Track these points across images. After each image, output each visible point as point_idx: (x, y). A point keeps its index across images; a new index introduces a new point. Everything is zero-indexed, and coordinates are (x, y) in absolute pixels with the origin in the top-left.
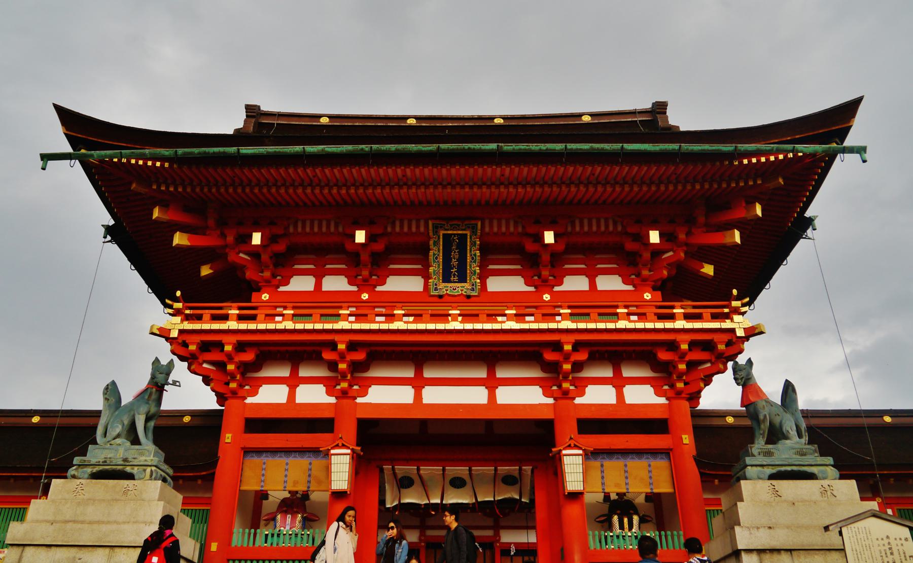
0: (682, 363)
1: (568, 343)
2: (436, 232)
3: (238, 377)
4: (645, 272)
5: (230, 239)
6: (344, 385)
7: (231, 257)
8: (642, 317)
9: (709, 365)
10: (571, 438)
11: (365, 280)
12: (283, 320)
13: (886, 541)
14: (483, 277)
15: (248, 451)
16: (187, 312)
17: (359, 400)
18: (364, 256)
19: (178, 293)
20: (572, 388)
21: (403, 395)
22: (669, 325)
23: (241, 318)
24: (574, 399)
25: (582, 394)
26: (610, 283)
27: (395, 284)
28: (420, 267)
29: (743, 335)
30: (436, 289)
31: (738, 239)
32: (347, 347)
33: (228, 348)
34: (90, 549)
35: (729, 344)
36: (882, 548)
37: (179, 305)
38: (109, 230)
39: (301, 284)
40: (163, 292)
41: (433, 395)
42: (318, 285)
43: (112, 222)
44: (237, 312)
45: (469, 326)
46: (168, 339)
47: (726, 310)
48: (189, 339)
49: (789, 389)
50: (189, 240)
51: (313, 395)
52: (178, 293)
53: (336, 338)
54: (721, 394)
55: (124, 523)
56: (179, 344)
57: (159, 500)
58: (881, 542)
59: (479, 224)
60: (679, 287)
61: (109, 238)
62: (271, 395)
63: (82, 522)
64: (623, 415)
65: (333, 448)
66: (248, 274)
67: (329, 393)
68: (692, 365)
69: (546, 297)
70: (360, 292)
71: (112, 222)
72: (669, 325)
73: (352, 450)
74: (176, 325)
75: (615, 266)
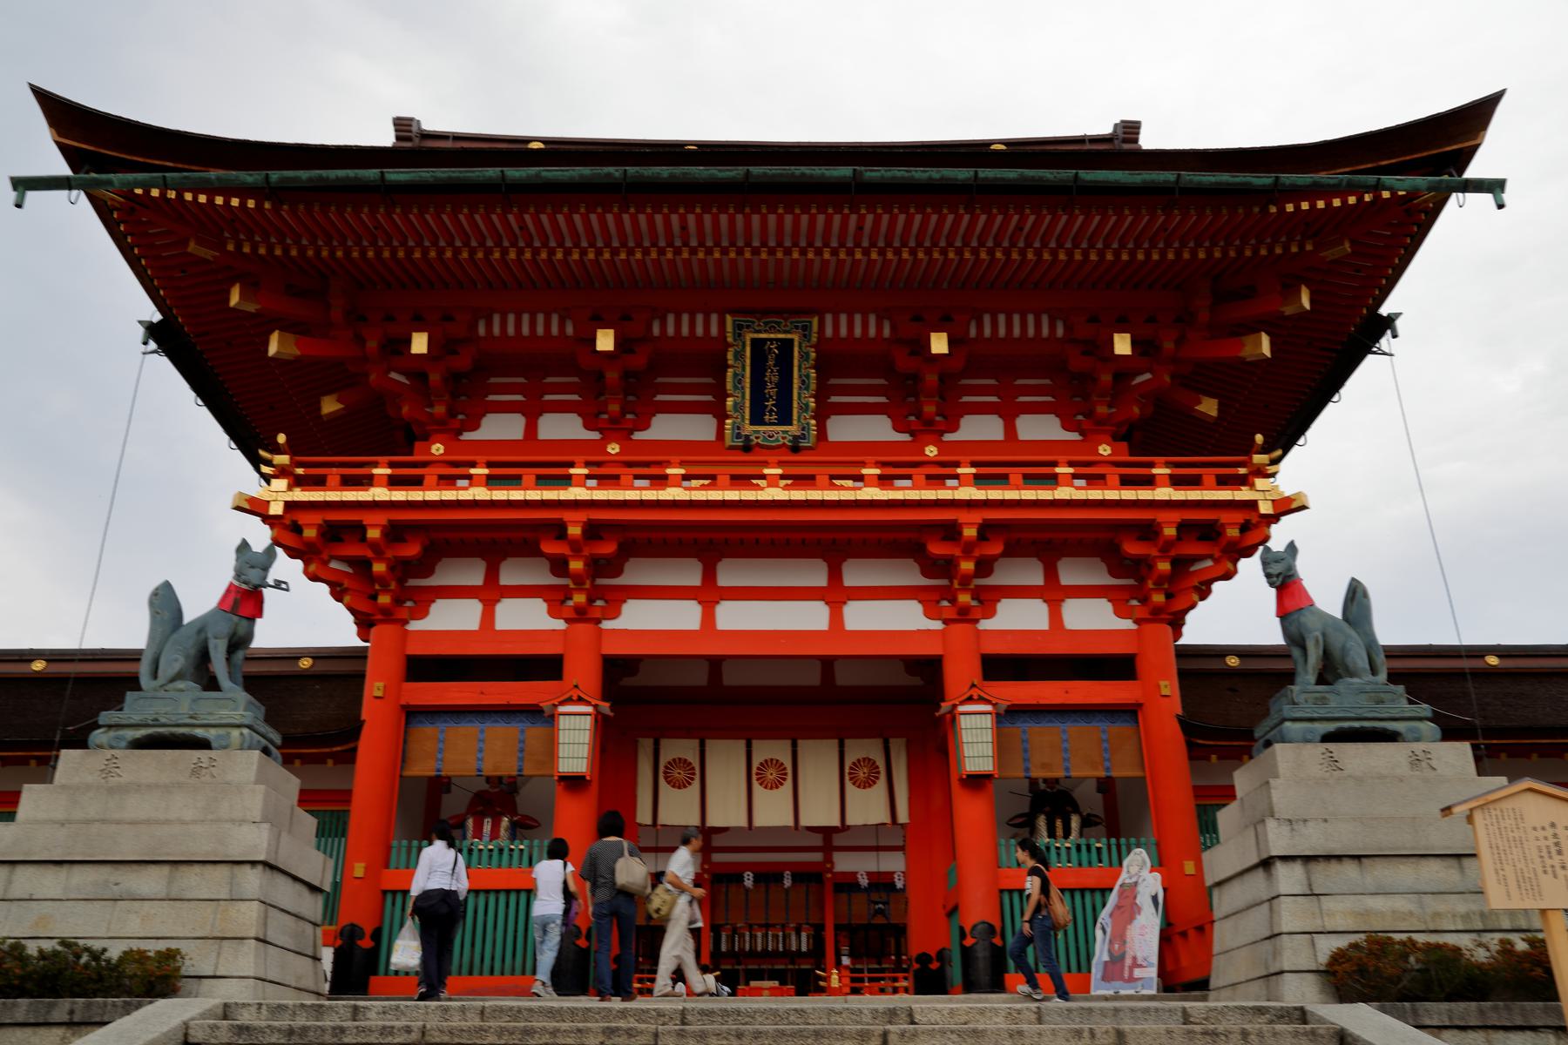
0: (1163, 558)
1: (970, 524)
2: (738, 336)
3: (393, 586)
4: (1102, 410)
5: (372, 344)
6: (580, 598)
7: (373, 377)
8: (1095, 480)
9: (1209, 563)
10: (973, 686)
11: (613, 420)
12: (471, 485)
13: (1550, 832)
14: (822, 415)
16: (300, 471)
17: (607, 625)
18: (612, 375)
19: (281, 438)
20: (974, 603)
21: (682, 616)
22: (1144, 494)
23: (393, 482)
24: (977, 621)
25: (991, 613)
26: (1040, 428)
27: (665, 428)
28: (709, 398)
29: (1271, 511)
30: (739, 436)
32: (584, 531)
33: (373, 534)
34: (135, 867)
35: (1245, 528)
36: (1543, 843)
37: (283, 459)
38: (152, 331)
39: (502, 428)
40: (250, 440)
41: (734, 617)
42: (531, 429)
44: (388, 471)
45: (798, 495)
46: (267, 519)
47: (1242, 471)
48: (303, 518)
49: (1356, 595)
50: (297, 344)
51: (525, 617)
52: (281, 438)
53: (567, 516)
54: (1234, 614)
55: (194, 822)
56: (285, 527)
57: (257, 782)
58: (1541, 834)
59: (815, 321)
60: (1156, 433)
61: (152, 345)
62: (451, 618)
63: (118, 822)
65: (562, 703)
66: (405, 409)
67: (553, 613)
69: (931, 451)
71: (157, 317)
72: (1144, 494)
73: (595, 706)
74: (279, 494)
75: (1049, 399)
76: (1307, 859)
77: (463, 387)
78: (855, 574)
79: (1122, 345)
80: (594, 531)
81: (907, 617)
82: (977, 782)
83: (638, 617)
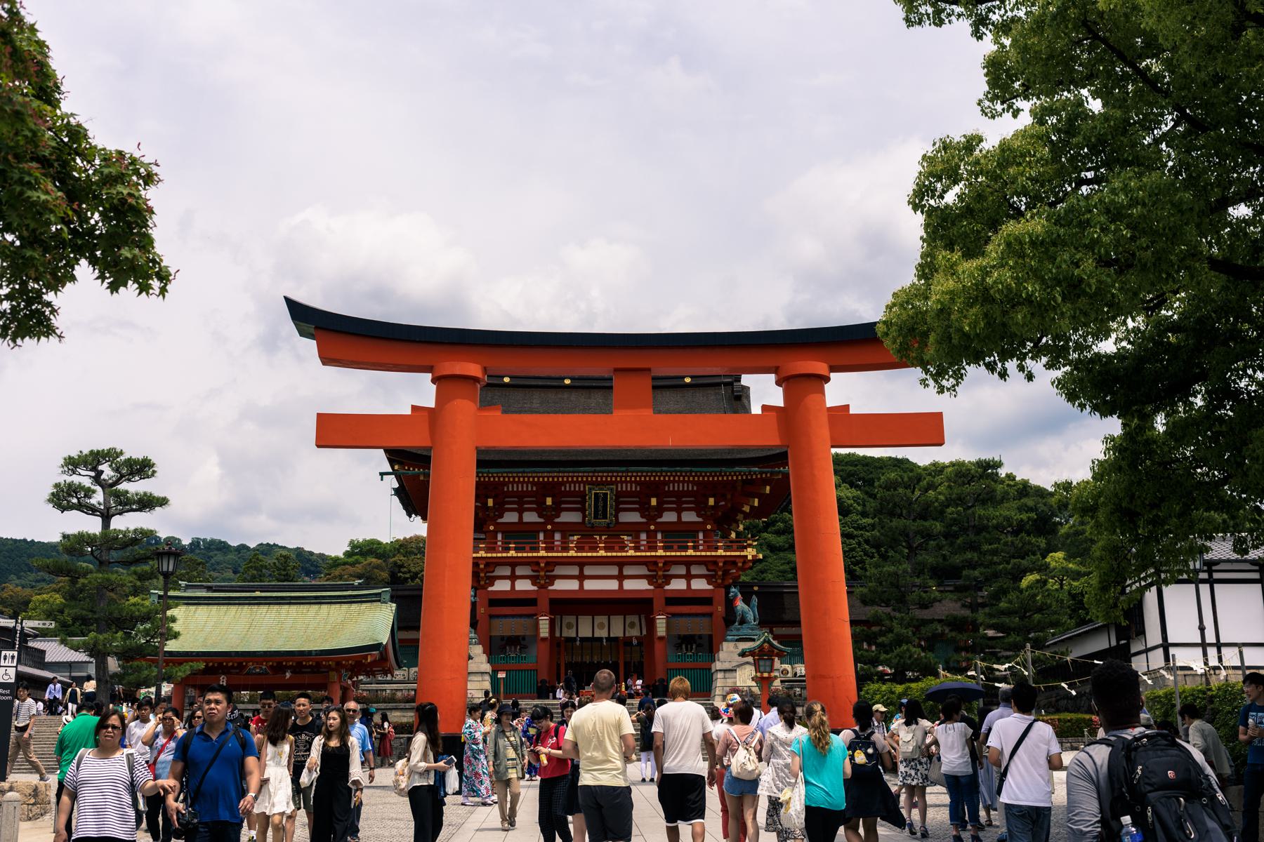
15: (491, 616)
21: (573, 585)
25: (669, 583)
26: (690, 517)
31: (756, 504)
35: (744, 563)
41: (590, 585)
42: (521, 518)
43: (396, 485)
51: (524, 586)
62: (502, 586)
64: (689, 595)
68: (726, 573)
69: (652, 527)
70: (545, 524)
71: (396, 485)
76: (725, 671)
77: (500, 510)
78: (628, 571)
79: (711, 501)
80: (547, 564)
81: (642, 585)
82: (661, 638)
83: (560, 585)
